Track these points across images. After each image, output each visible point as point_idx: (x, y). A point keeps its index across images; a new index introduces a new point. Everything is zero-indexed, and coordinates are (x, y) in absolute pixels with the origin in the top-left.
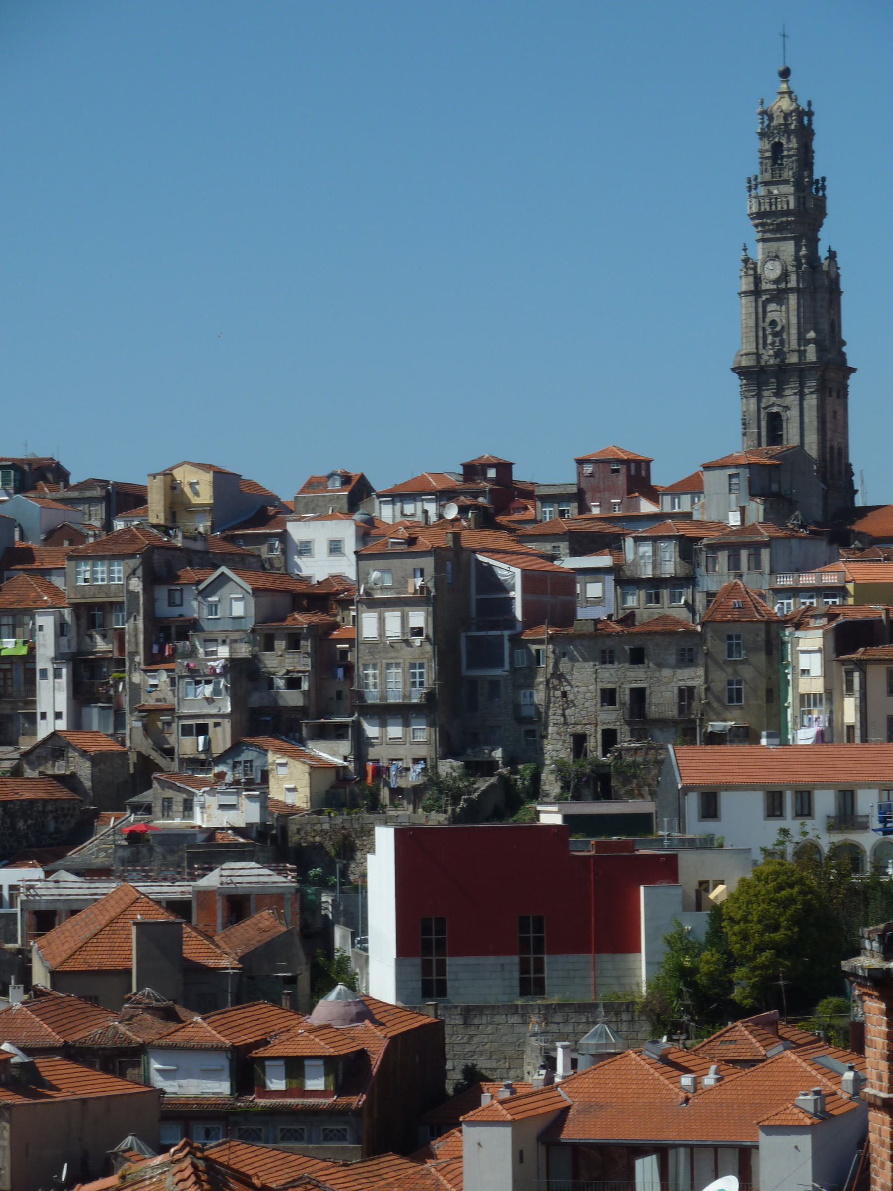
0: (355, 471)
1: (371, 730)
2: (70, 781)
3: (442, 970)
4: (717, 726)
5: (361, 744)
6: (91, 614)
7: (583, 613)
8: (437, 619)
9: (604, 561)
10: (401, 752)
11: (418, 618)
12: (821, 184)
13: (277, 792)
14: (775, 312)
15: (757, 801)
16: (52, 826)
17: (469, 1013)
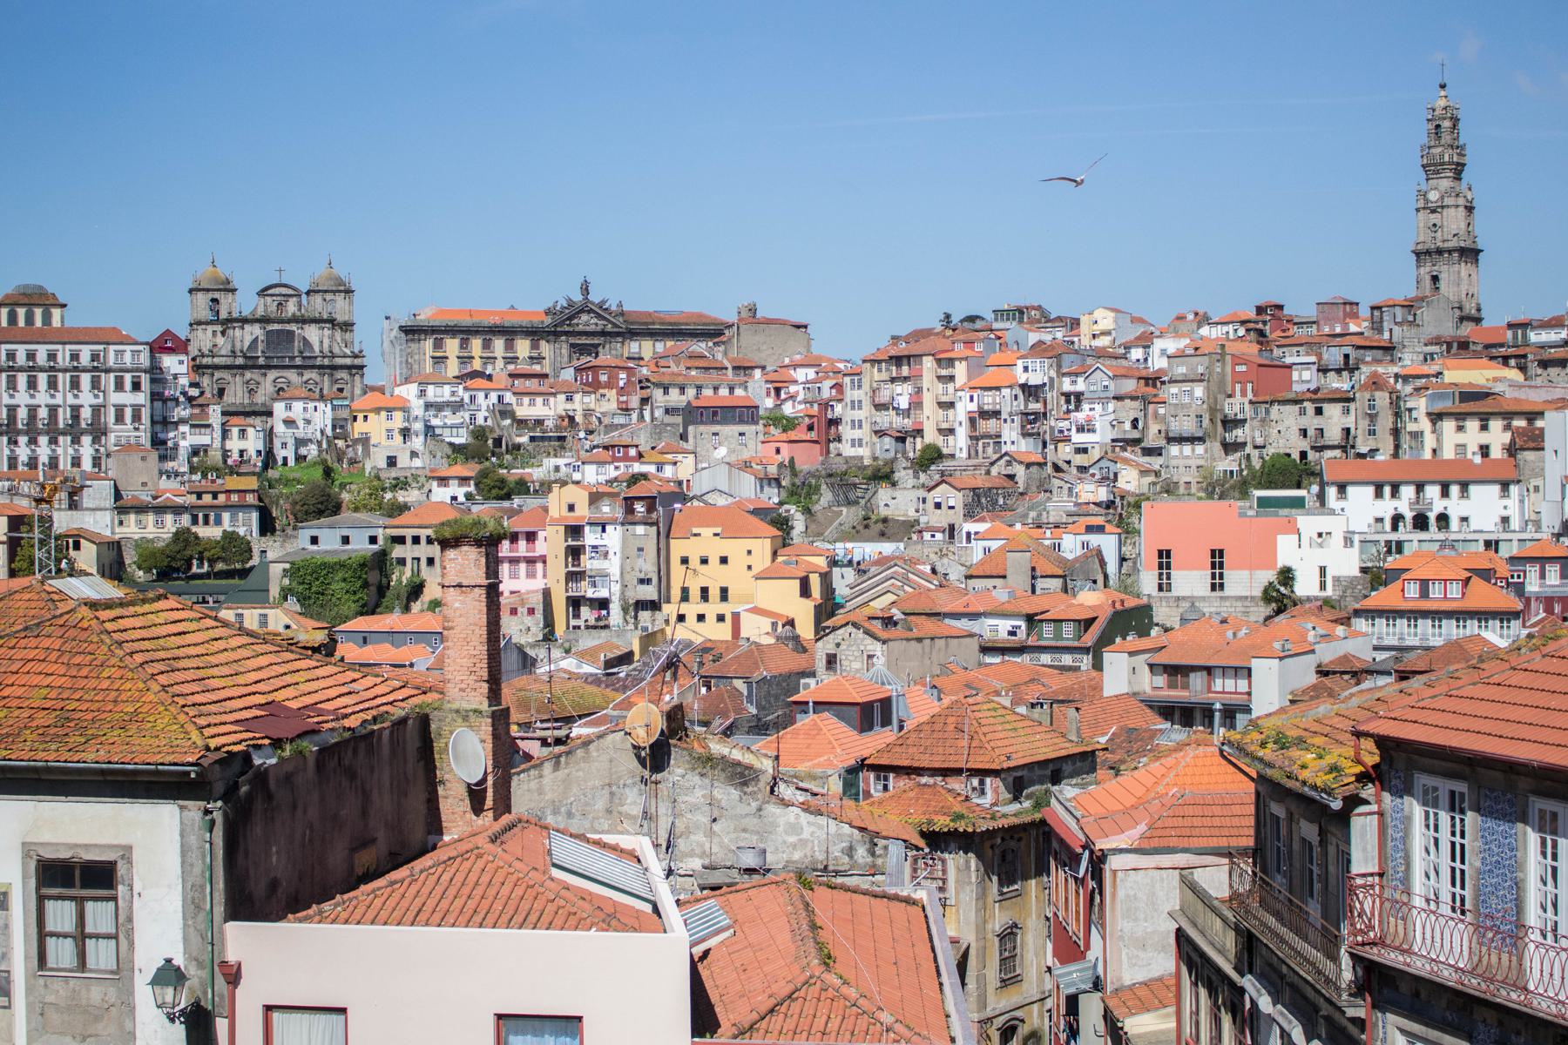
0: (1201, 312)
1: (1174, 450)
2: (1011, 477)
3: (1169, 578)
4: (1364, 450)
5: (1169, 458)
6: (1031, 391)
7: (1296, 388)
8: (1208, 389)
9: (1313, 359)
10: (1189, 462)
11: (1199, 391)
12: (1462, 147)
13: (1121, 484)
14: (1435, 218)
15: (1371, 490)
16: (1001, 501)
17: (1178, 599)
